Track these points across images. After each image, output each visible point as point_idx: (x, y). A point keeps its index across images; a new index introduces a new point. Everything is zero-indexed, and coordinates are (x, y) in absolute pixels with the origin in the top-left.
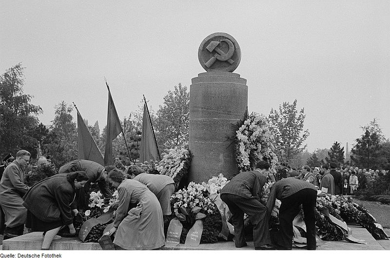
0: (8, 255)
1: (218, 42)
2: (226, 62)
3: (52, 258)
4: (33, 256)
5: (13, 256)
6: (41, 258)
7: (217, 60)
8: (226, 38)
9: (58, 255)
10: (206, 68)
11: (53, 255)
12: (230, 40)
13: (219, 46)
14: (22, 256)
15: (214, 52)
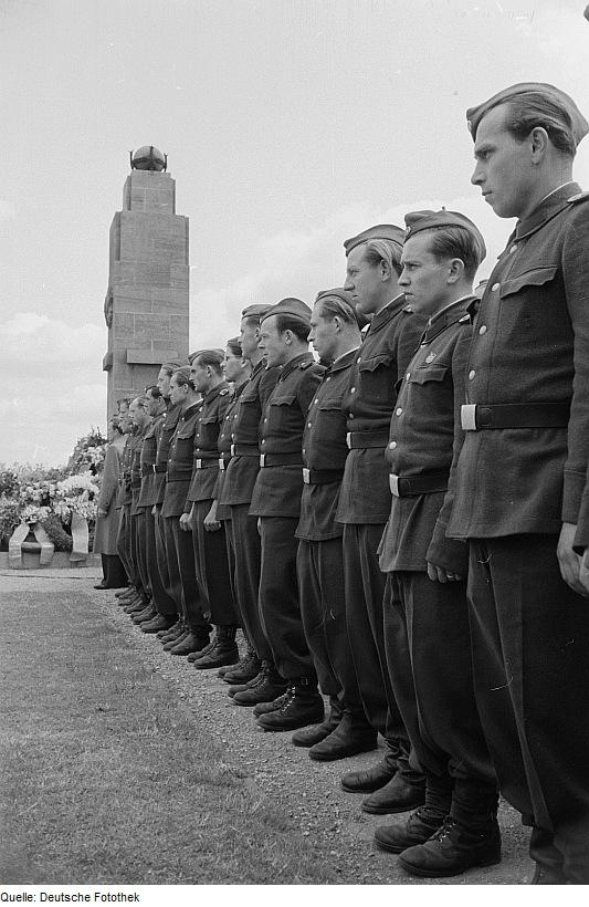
0: (19, 897)
3: (117, 904)
4: (75, 898)
5: (29, 898)
6: (92, 903)
9: (130, 897)
11: (120, 897)
14: (50, 898)
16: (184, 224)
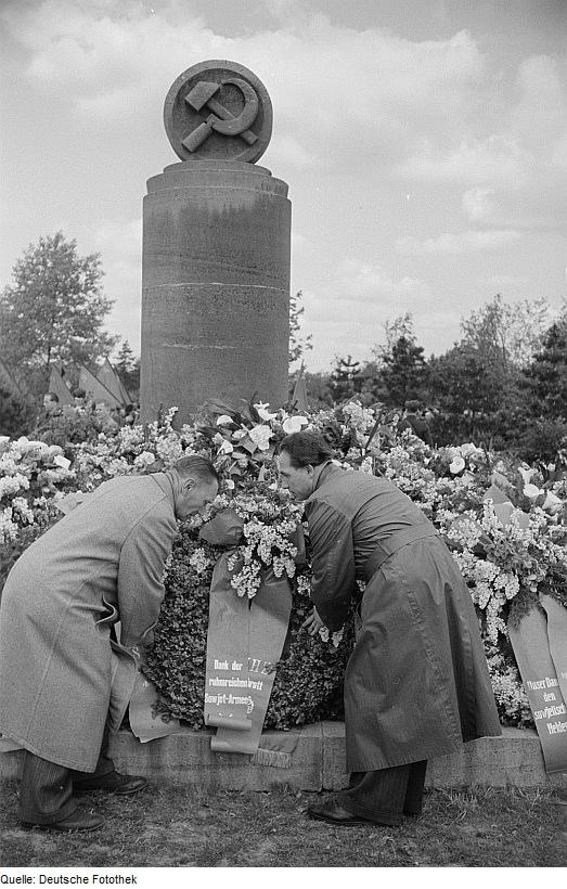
0: (19, 879)
1: (215, 86)
2: (238, 137)
4: (73, 880)
5: (28, 880)
7: (214, 133)
8: (235, 74)
9: (128, 879)
10: (184, 152)
11: (118, 879)
12: (247, 80)
13: (216, 95)
14: (50, 880)
15: (206, 110)
16: (282, 188)
